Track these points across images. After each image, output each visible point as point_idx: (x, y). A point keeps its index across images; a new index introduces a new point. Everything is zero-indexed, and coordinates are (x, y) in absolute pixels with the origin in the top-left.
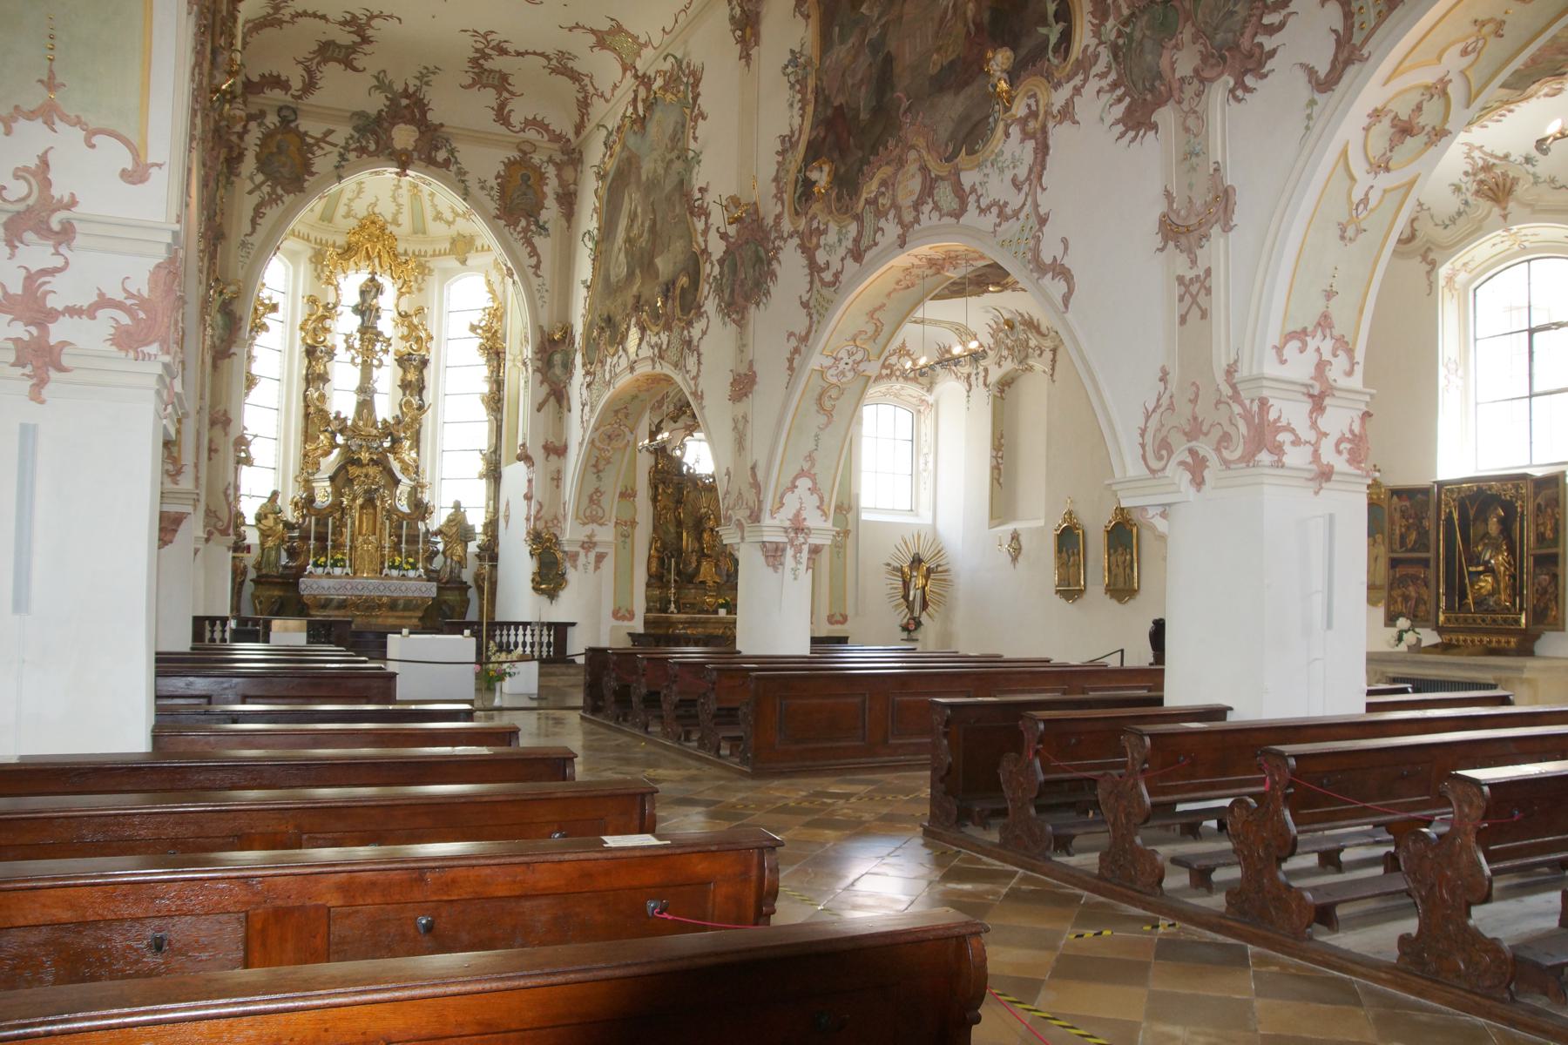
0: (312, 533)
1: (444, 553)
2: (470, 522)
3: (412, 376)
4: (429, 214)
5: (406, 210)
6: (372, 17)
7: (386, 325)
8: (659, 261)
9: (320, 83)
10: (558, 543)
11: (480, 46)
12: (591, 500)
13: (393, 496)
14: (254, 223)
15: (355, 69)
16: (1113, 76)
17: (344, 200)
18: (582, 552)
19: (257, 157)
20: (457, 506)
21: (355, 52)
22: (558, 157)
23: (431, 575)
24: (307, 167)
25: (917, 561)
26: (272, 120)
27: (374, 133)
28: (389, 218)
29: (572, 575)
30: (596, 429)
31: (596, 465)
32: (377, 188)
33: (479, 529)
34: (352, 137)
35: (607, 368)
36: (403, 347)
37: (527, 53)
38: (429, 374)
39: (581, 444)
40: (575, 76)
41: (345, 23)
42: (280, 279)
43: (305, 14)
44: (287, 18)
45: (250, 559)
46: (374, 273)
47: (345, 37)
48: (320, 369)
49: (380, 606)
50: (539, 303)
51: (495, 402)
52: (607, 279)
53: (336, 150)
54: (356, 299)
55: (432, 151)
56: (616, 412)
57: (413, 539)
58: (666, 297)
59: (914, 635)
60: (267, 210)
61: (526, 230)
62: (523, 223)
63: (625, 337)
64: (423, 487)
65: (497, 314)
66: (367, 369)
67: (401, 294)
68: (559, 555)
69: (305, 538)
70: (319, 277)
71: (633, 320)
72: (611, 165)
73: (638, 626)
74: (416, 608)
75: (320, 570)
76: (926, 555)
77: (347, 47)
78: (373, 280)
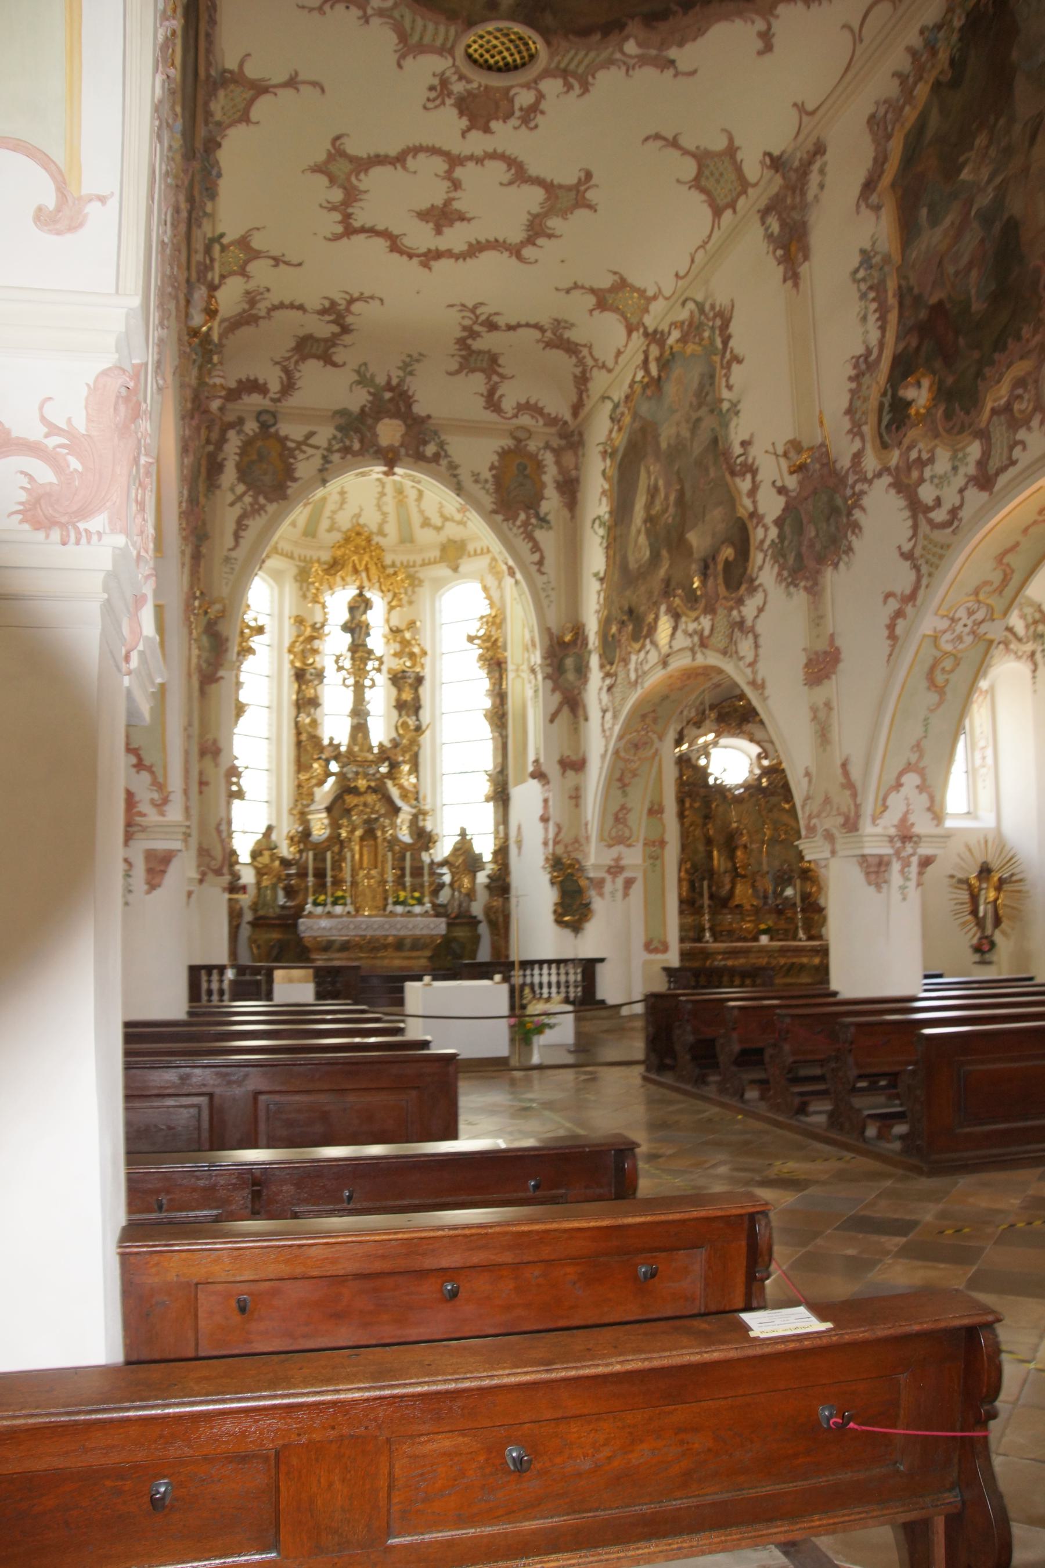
0: (306, 871)
1: (451, 885)
2: (477, 849)
3: (407, 696)
4: (416, 520)
5: (392, 519)
6: (351, 301)
7: (377, 642)
8: (693, 537)
9: (299, 384)
10: (582, 869)
11: (467, 322)
12: (617, 819)
13: (393, 825)
14: (237, 537)
15: (335, 365)
17: (327, 513)
18: (609, 878)
19: (238, 466)
20: (463, 834)
21: (334, 345)
22: (556, 442)
23: (439, 911)
24: (289, 473)
26: (251, 427)
27: (357, 430)
28: (374, 528)
29: (598, 904)
30: (620, 738)
31: (620, 778)
32: (361, 493)
33: (487, 857)
34: (335, 437)
35: (632, 666)
36: (396, 664)
37: (519, 325)
38: (425, 691)
39: (603, 756)
40: (571, 348)
41: (323, 312)
42: (264, 599)
43: (281, 306)
44: (263, 313)
45: (245, 900)
46: (361, 588)
47: (324, 329)
48: (310, 693)
49: (385, 947)
50: (545, 603)
51: (499, 717)
52: (624, 567)
53: (319, 453)
54: (345, 616)
55: (420, 444)
56: (644, 717)
57: (417, 871)
58: (704, 576)
59: (987, 956)
60: (250, 522)
61: (526, 524)
62: (522, 516)
63: (652, 629)
64: (425, 813)
65: (496, 621)
66: (359, 689)
67: (391, 608)
68: (583, 883)
69: (302, 875)
70: (304, 596)
71: (663, 608)
72: (620, 440)
73: (673, 959)
74: (425, 947)
75: (319, 910)
76: (995, 865)
77: (326, 340)
78: (361, 595)
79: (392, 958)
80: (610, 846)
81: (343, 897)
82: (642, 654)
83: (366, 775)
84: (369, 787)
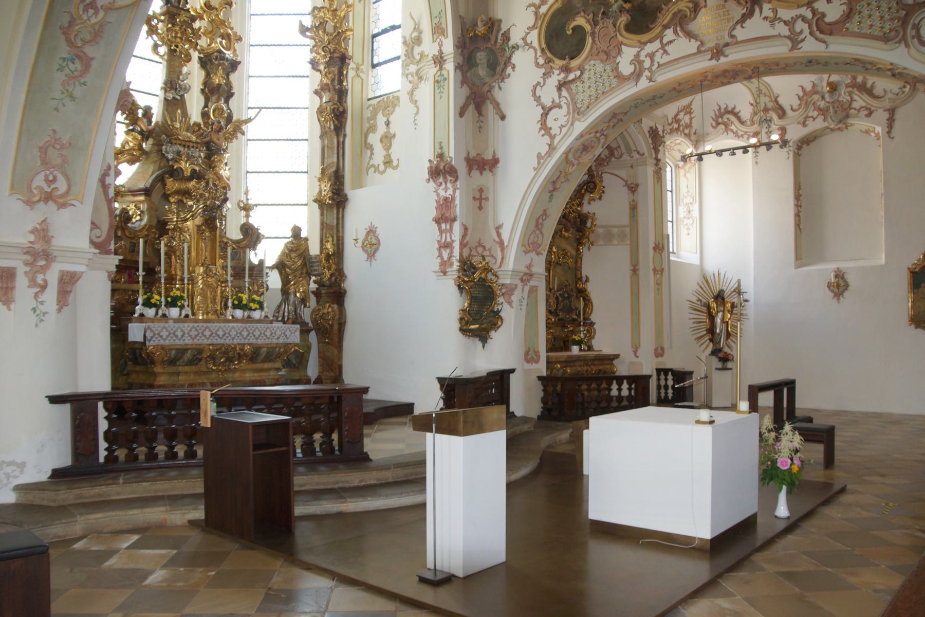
12: (537, 225)
18: (520, 284)
25: (720, 297)
30: (581, 135)
79: (244, 371)
80: (526, 252)
81: (182, 298)
82: (650, 48)
83: (189, 158)
84: (194, 171)
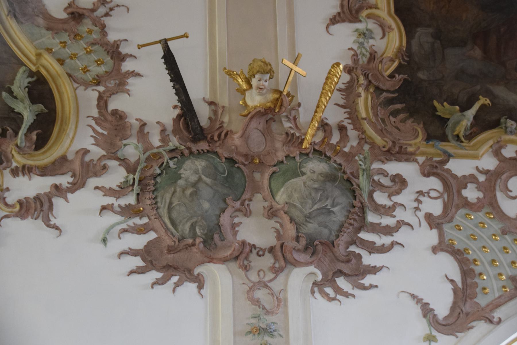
16: (130, 199)
